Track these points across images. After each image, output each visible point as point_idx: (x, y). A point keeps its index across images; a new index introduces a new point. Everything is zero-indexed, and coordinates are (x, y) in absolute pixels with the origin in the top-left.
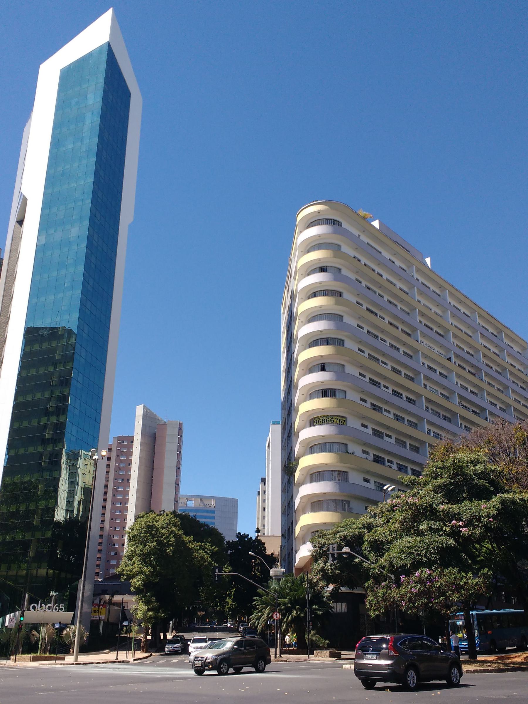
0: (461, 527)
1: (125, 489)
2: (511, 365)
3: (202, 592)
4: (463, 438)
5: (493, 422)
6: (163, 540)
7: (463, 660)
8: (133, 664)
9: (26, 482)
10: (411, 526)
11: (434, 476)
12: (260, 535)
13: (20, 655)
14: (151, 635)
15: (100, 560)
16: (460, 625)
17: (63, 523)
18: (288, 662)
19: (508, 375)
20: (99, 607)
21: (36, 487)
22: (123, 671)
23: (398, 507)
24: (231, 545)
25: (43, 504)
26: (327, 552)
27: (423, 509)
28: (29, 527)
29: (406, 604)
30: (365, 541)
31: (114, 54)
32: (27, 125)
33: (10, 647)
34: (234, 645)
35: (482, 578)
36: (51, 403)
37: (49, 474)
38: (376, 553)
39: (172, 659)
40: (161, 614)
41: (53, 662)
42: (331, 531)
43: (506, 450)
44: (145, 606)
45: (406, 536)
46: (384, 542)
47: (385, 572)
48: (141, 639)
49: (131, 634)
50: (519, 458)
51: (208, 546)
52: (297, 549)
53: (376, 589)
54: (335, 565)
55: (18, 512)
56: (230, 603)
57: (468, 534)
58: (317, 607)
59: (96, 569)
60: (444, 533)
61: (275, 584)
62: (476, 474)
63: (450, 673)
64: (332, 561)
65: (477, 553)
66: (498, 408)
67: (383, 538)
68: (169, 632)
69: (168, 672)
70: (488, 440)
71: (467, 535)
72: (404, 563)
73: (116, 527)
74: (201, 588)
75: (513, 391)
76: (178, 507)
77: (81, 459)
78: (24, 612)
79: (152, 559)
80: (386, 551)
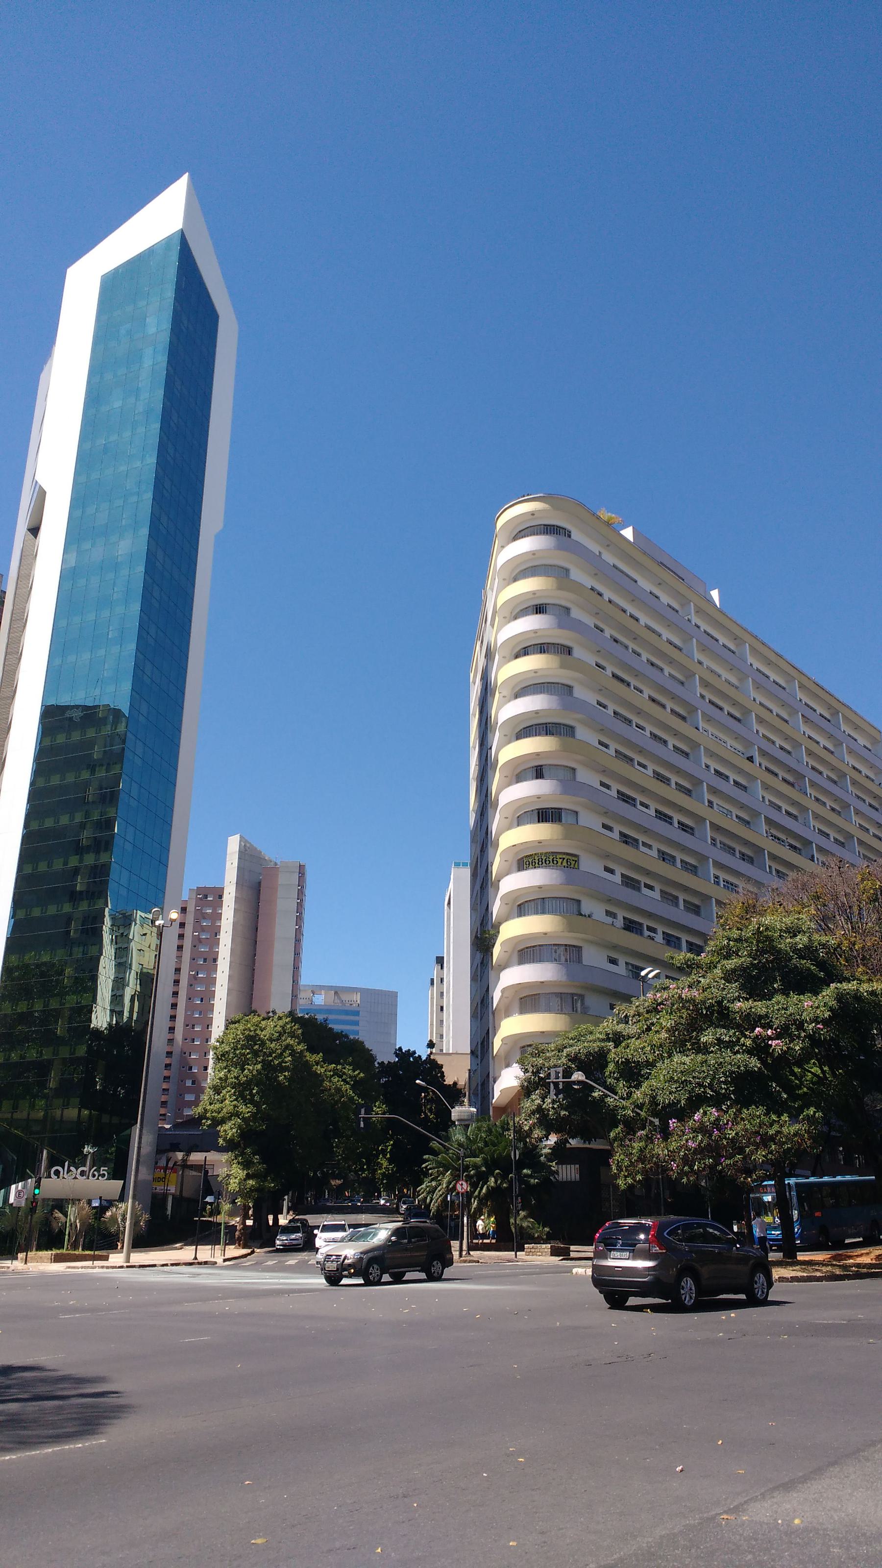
0: (770, 1038)
1: (209, 974)
2: (854, 768)
3: (337, 1147)
4: (773, 890)
5: (824, 864)
6: (272, 1061)
7: (774, 1260)
8: (222, 1266)
9: (45, 964)
10: (687, 1038)
11: (725, 953)
12: (434, 1051)
13: (34, 1253)
14: (252, 1218)
15: (169, 1082)
16: (768, 1202)
17: (105, 1031)
18: (481, 1263)
19: (849, 786)
20: (165, 1172)
21: (61, 973)
22: (206, 1278)
23: (665, 1005)
24: (387, 1068)
25: (71, 1000)
26: (547, 1081)
27: (707, 1009)
28: (49, 1039)
29: (678, 1166)
30: (610, 1062)
31: (190, 249)
32: (46, 368)
33: (17, 1238)
34: (392, 1235)
35: (805, 1123)
36: (85, 831)
37: (82, 950)
38: (629, 1082)
39: (288, 1258)
40: (270, 1183)
41: (89, 1263)
42: (553, 1045)
43: (845, 910)
44: (243, 1169)
45: (679, 1054)
46: (642, 1063)
47: (643, 1114)
48: (236, 1226)
49: (218, 1217)
50: (866, 924)
51: (348, 1070)
52: (497, 1075)
53: (628, 1143)
54: (559, 1101)
55: (31, 1014)
56: (384, 1166)
57: (782, 1050)
58: (529, 1172)
59: (161, 1109)
60: (742, 1048)
61: (459, 1134)
62: (795, 950)
63: (752, 1282)
64: (555, 1095)
65: (798, 1082)
66: (832, 840)
67: (639, 1058)
68: (282, 1214)
69: (281, 1281)
70: (815, 894)
71: (780, 1052)
72: (675, 1099)
73: (194, 1039)
74: (336, 1140)
75: (857, 812)
76: (298, 1005)
77: (135, 925)
78: (41, 1180)
79: (254, 1091)
80: (645, 1079)
